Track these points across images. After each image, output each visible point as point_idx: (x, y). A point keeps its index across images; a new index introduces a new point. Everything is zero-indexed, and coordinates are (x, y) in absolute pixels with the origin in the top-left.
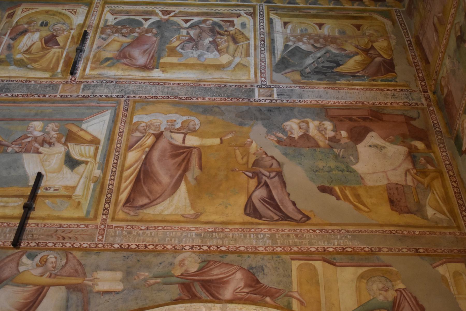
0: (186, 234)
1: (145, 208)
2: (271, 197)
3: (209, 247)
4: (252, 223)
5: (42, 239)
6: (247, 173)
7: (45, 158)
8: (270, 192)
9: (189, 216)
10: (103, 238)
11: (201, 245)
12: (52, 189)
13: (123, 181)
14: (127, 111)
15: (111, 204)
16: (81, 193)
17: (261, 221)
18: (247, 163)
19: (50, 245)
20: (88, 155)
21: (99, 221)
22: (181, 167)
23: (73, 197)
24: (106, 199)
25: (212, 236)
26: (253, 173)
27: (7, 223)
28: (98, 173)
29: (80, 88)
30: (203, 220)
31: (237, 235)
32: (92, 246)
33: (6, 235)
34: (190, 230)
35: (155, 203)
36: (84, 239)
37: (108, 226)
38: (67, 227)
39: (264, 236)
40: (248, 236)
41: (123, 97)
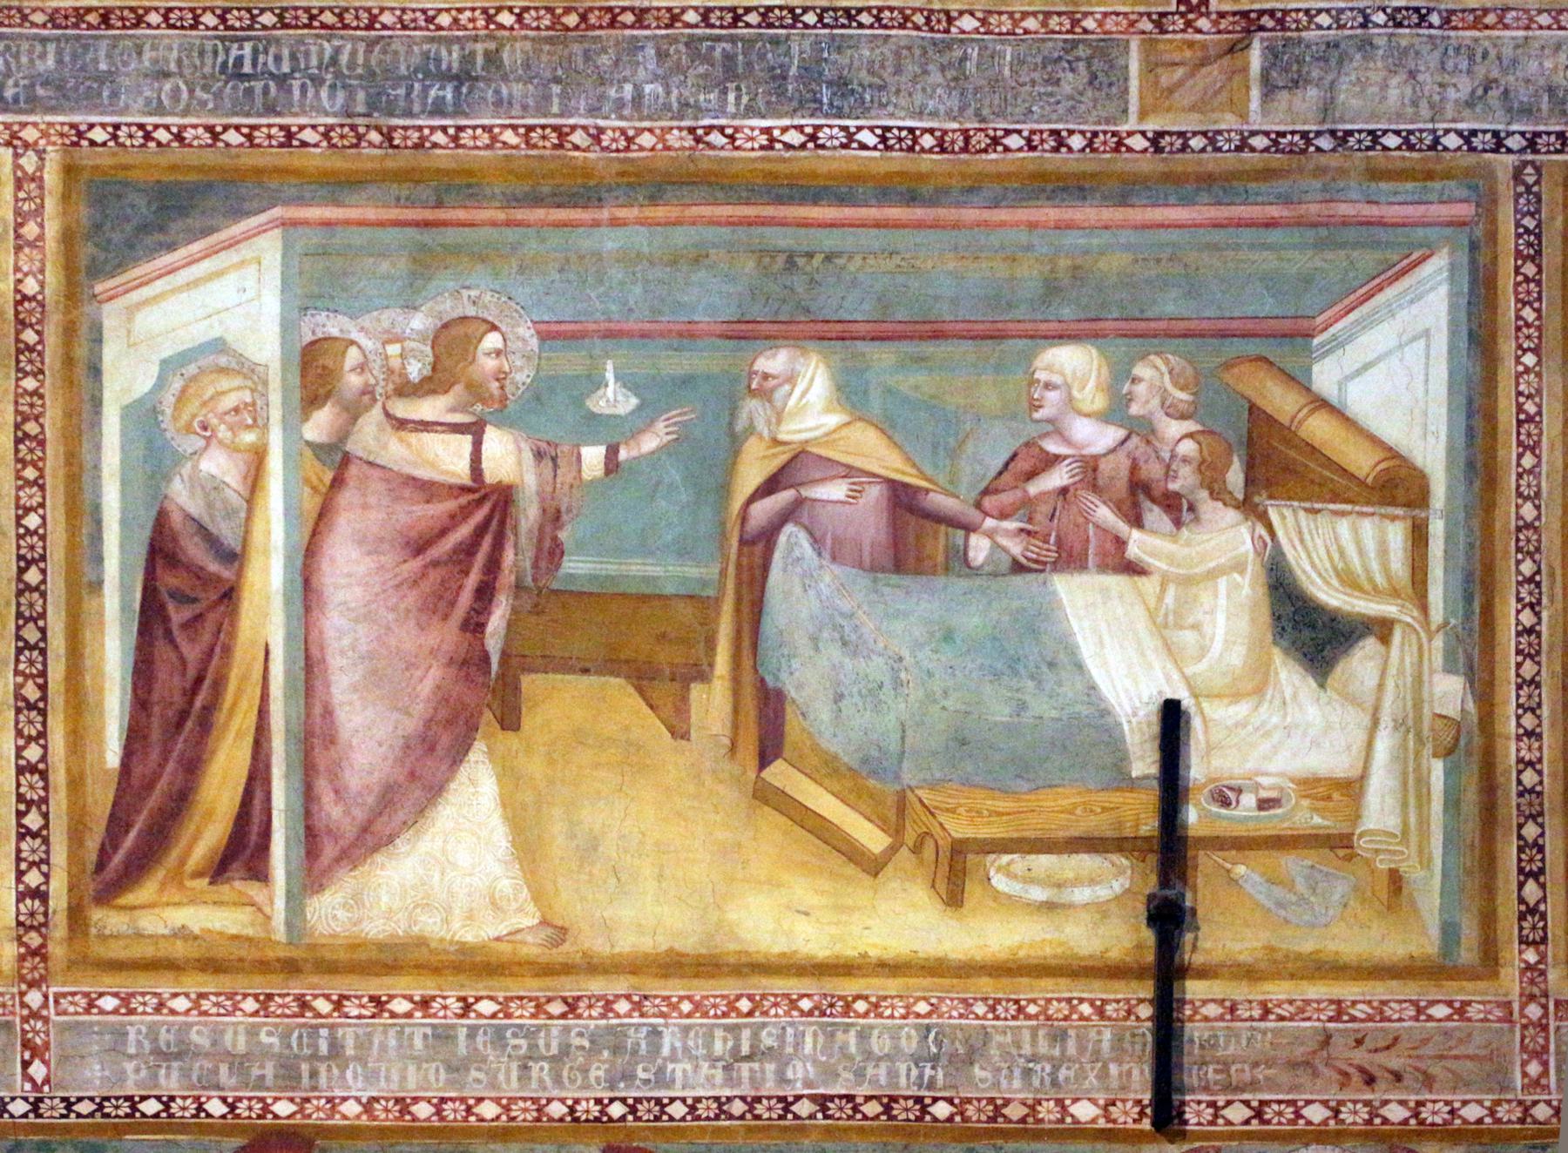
5: (1272, 1085)
7: (1169, 599)
10: (1545, 1073)
12: (1249, 800)
14: (1536, 258)
15: (1547, 878)
16: (1392, 822)
19: (1316, 1114)
20: (1380, 580)
21: (1511, 982)
23: (1363, 845)
24: (1520, 850)
27: (1092, 1003)
28: (1449, 692)
29: (1245, 69)
32: (1502, 1112)
33: (1105, 1067)
36: (1459, 1082)
37: (1557, 1003)
38: (1370, 1019)
41: (1499, 145)
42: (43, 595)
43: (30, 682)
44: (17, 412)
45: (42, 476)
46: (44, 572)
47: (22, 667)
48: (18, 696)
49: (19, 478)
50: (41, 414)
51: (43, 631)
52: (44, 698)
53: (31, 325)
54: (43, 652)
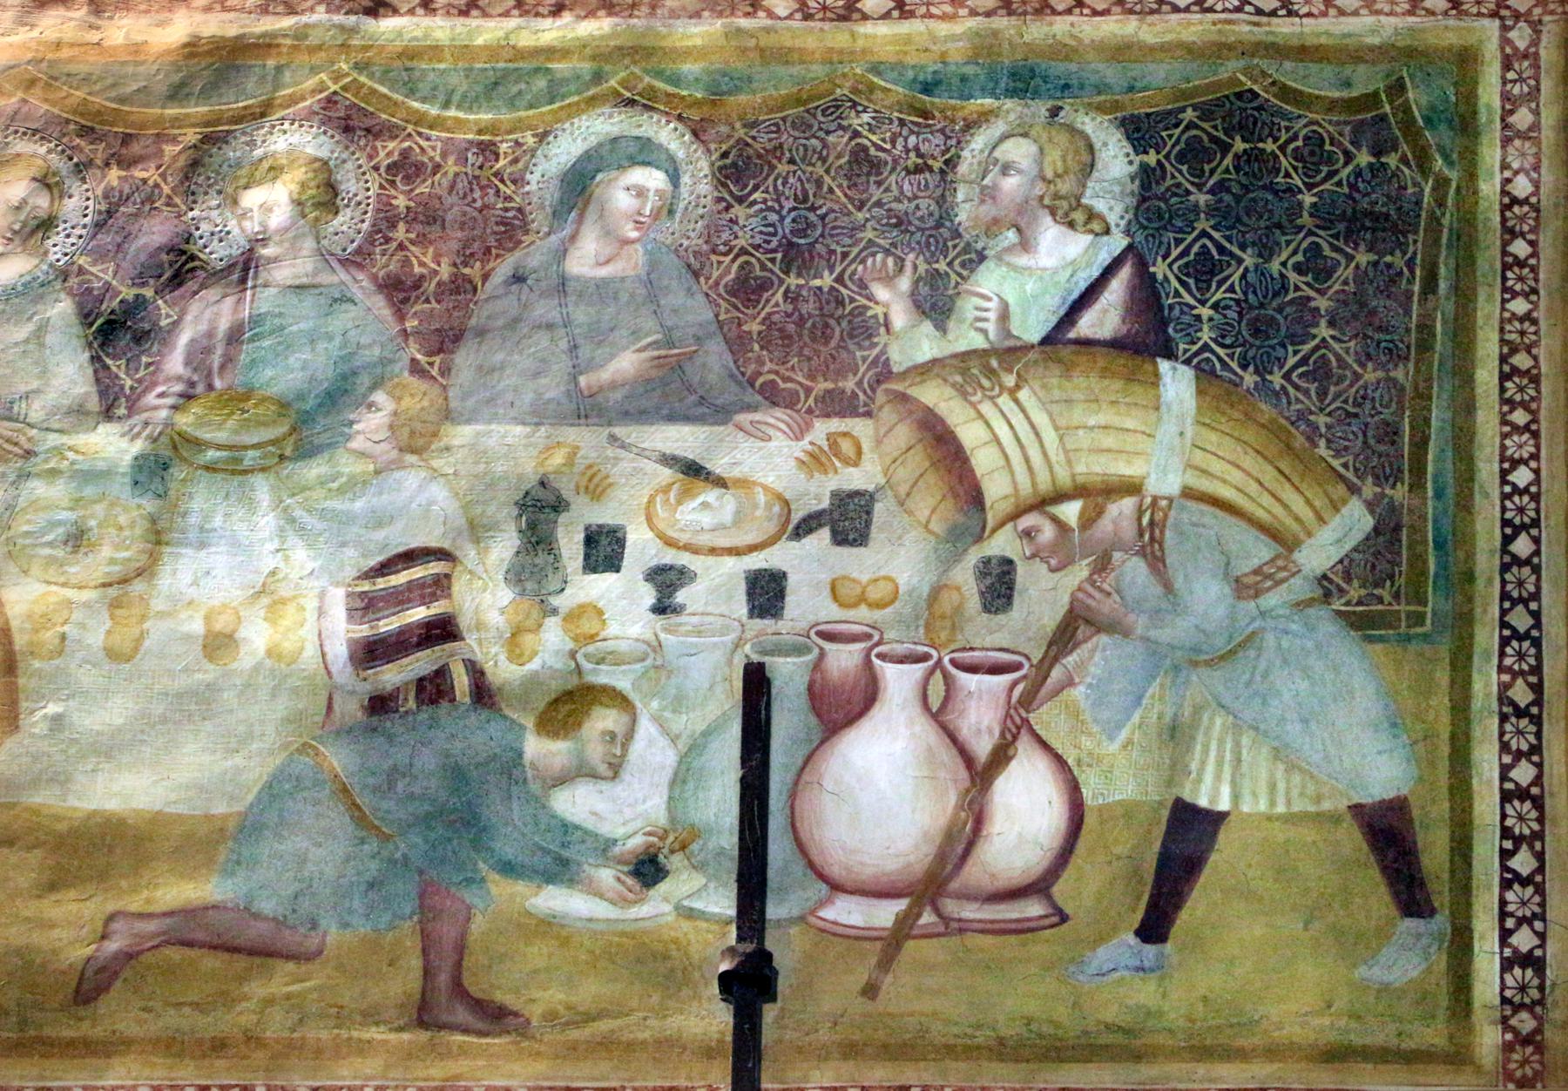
42: (1536, 570)
43: (1520, 681)
44: (1502, 341)
45: (1535, 421)
46: (1537, 541)
47: (1508, 661)
48: (1503, 699)
49: (1504, 422)
50: (1535, 344)
51: (1536, 615)
52: (1538, 702)
53: (1522, 235)
54: (1537, 643)
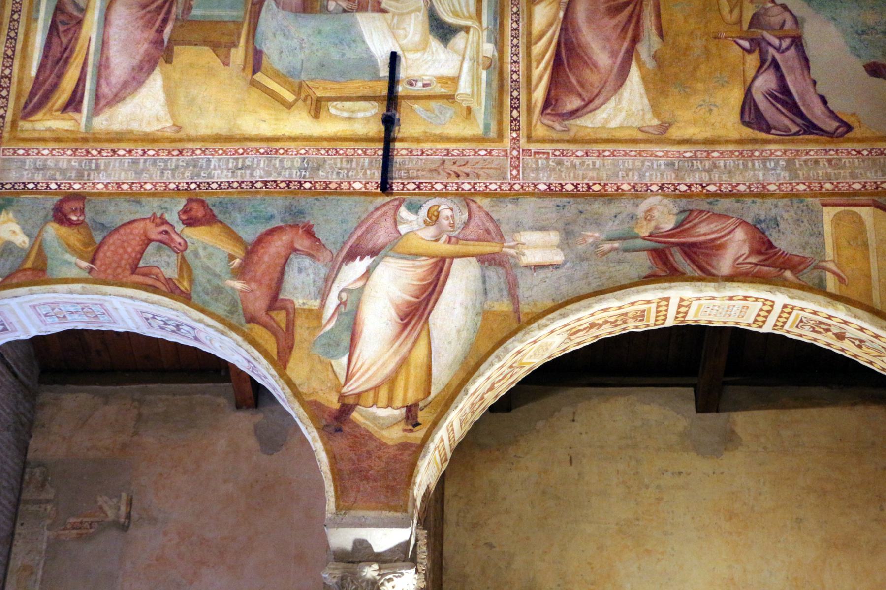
0: (649, 164)
1: (578, 117)
2: (784, 89)
3: (689, 187)
4: (754, 141)
6: (742, 42)
8: (781, 78)
9: (651, 130)
11: (676, 182)
13: (534, 64)
17: (771, 137)
18: (740, 21)
22: (626, 33)
25: (692, 166)
26: (751, 41)
30: (674, 137)
31: (732, 164)
34: (656, 156)
35: (592, 106)
39: (777, 163)
40: (750, 164)
